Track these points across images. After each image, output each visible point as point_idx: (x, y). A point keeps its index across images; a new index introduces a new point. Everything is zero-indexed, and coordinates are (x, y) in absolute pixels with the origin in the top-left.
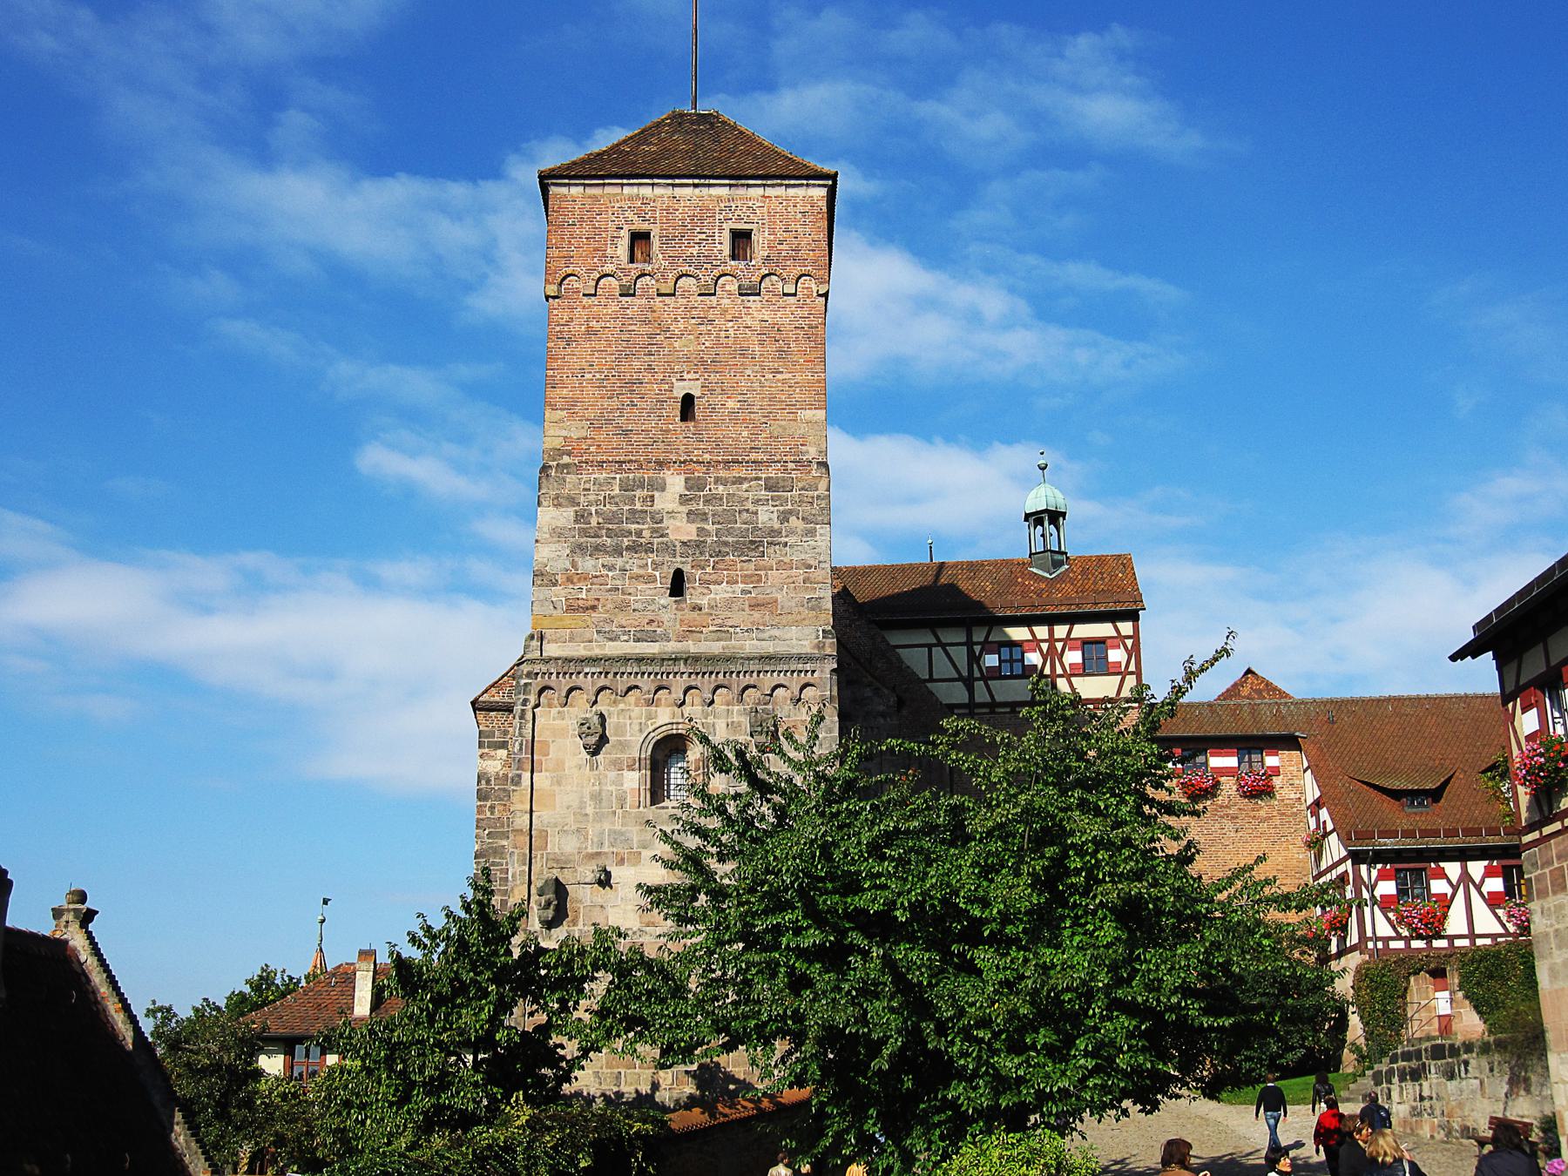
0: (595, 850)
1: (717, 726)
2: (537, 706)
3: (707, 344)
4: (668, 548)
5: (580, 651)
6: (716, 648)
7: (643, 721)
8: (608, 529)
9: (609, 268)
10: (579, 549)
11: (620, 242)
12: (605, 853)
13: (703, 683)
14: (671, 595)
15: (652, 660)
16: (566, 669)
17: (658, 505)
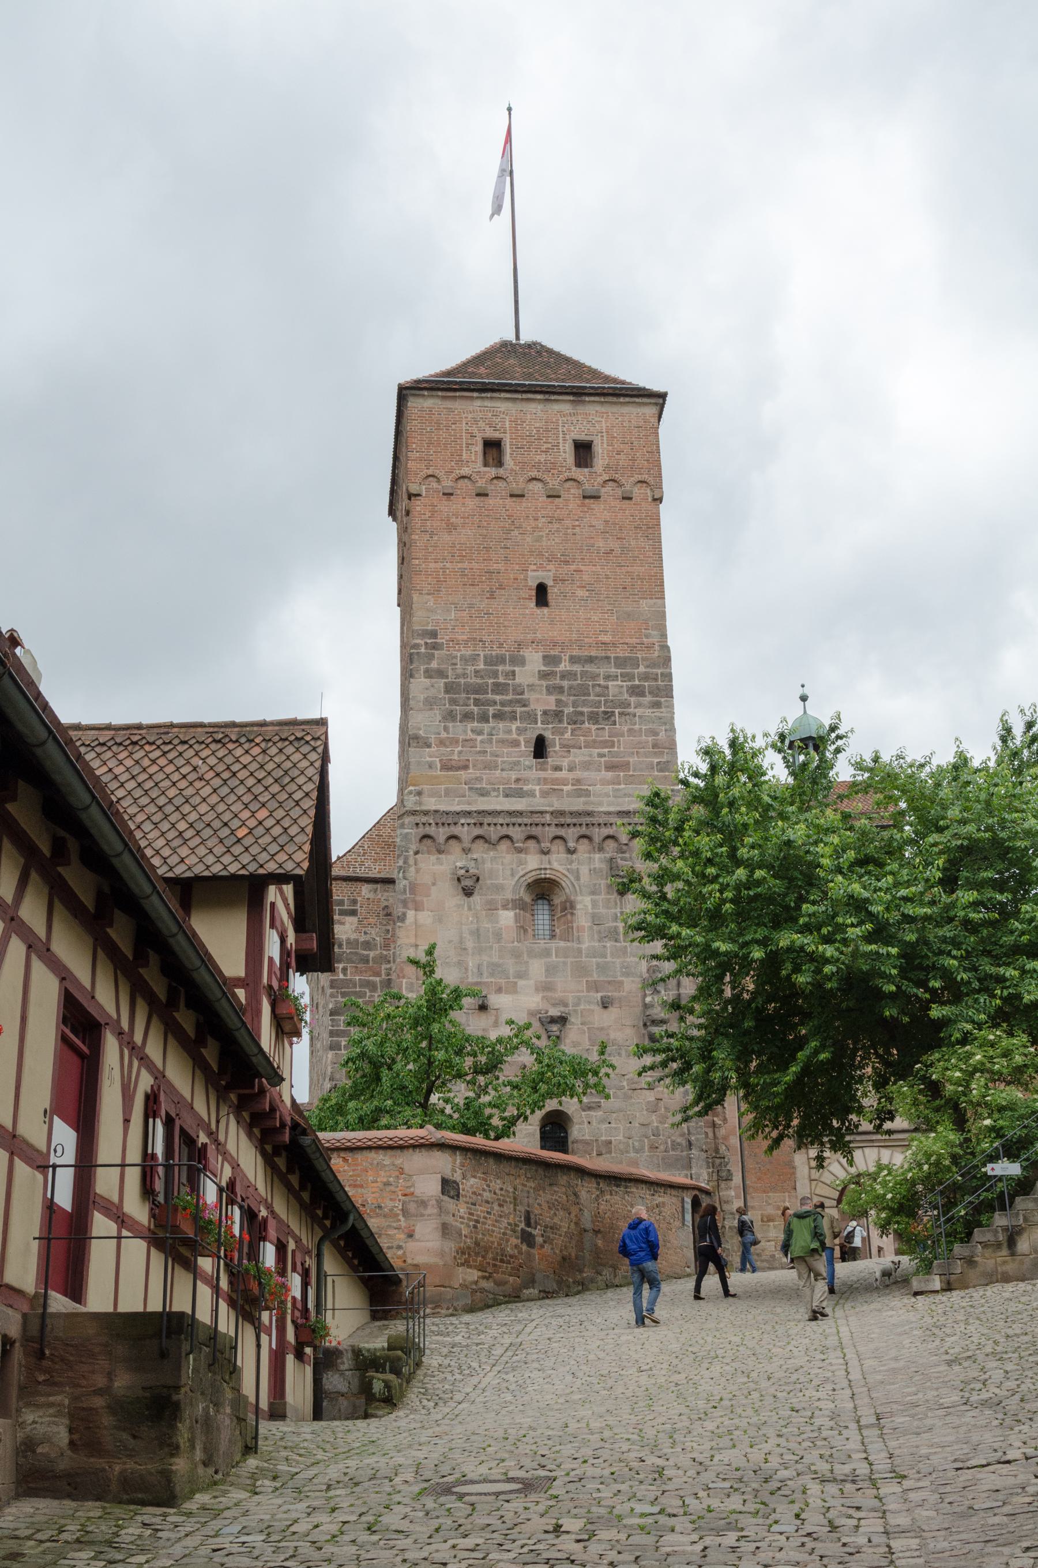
0: (475, 980)
1: (581, 872)
2: (417, 853)
3: (557, 541)
4: (531, 717)
5: (456, 806)
6: (578, 804)
7: (514, 866)
8: (475, 699)
9: (465, 471)
10: (450, 716)
11: (473, 449)
12: (485, 983)
13: (567, 833)
14: (535, 757)
15: (520, 813)
16: (444, 820)
17: (518, 681)
